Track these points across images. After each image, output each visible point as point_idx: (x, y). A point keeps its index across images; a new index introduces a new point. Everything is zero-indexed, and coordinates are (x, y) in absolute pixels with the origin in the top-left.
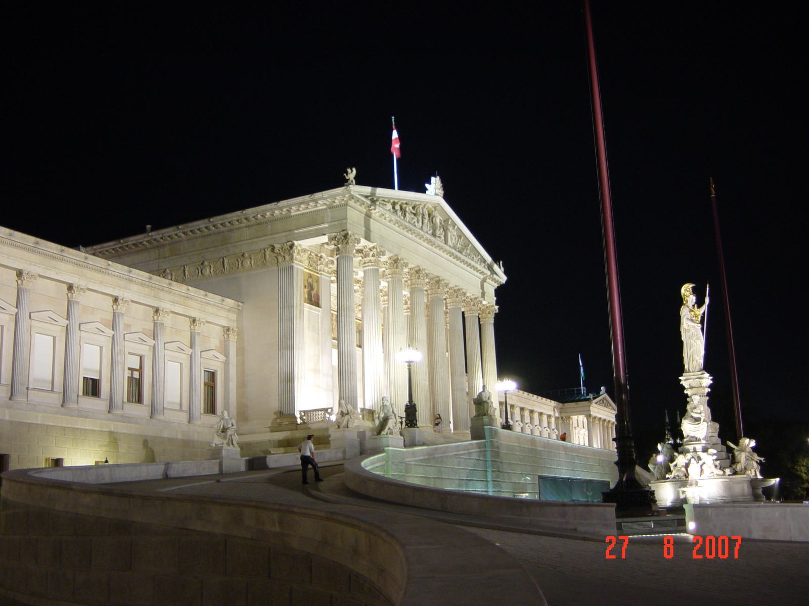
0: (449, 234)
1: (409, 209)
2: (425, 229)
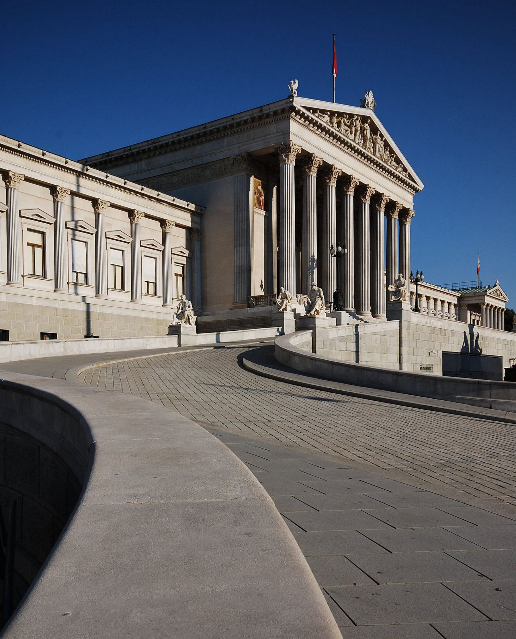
1: (344, 121)
2: (357, 141)
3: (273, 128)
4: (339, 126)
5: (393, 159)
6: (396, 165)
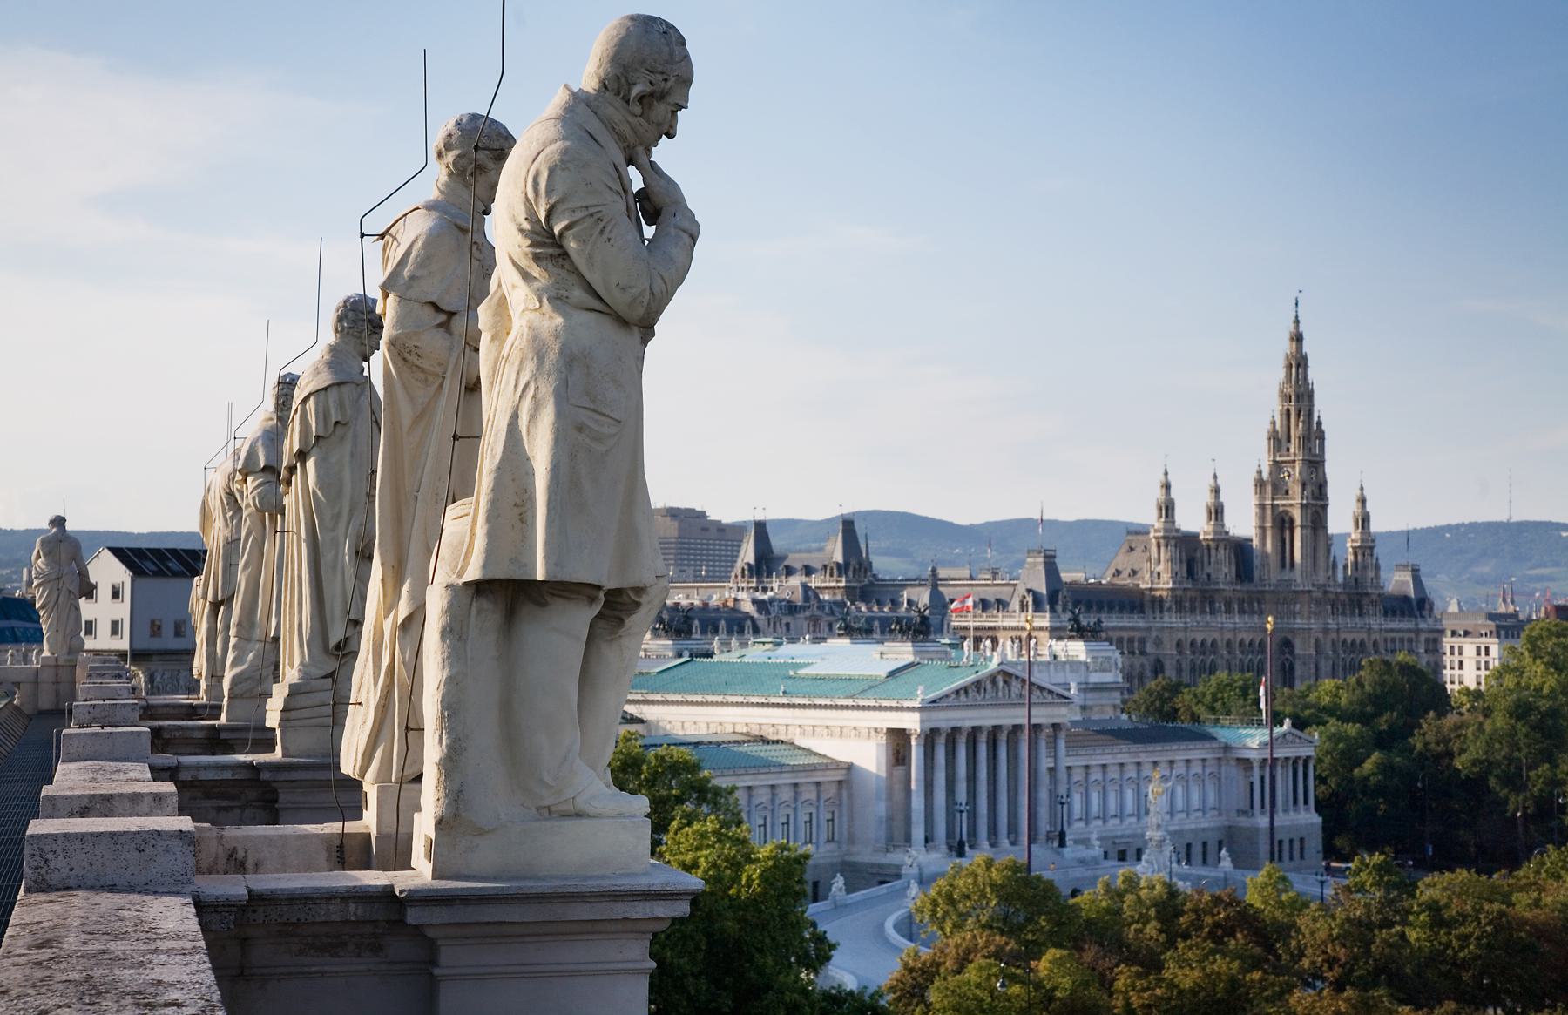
6: (1038, 693)
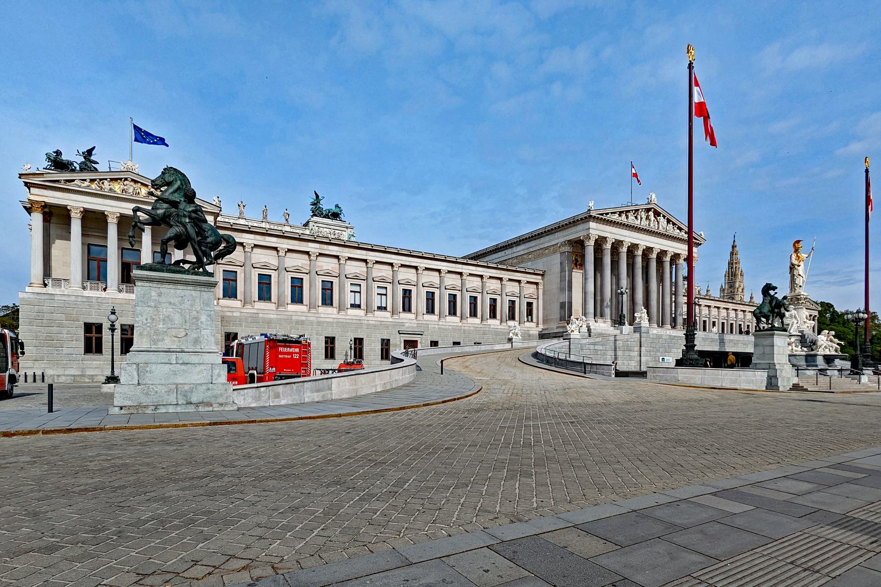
0: (660, 223)
3: (581, 227)
4: (627, 218)
5: (676, 228)
6: (678, 231)
